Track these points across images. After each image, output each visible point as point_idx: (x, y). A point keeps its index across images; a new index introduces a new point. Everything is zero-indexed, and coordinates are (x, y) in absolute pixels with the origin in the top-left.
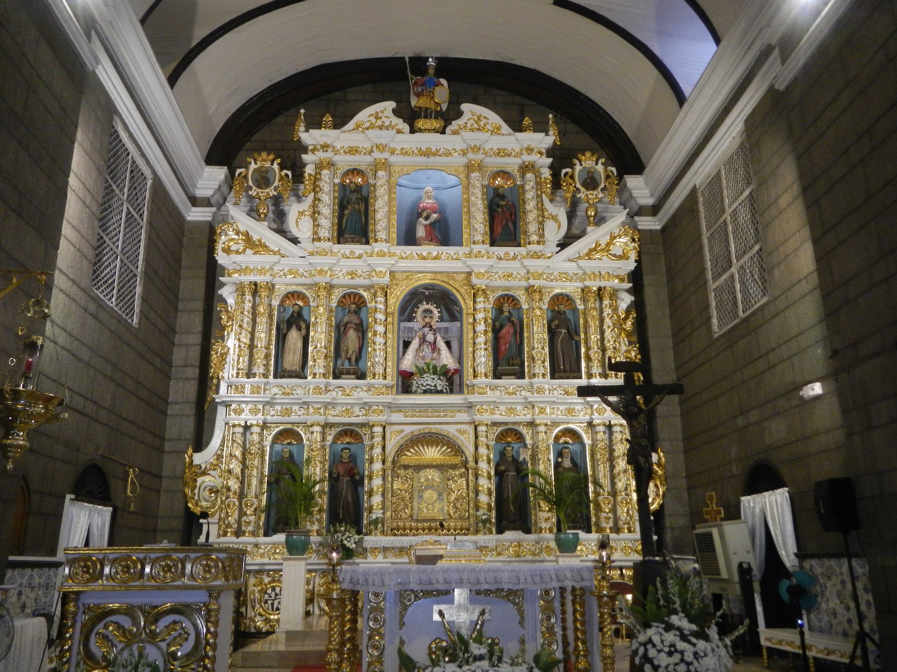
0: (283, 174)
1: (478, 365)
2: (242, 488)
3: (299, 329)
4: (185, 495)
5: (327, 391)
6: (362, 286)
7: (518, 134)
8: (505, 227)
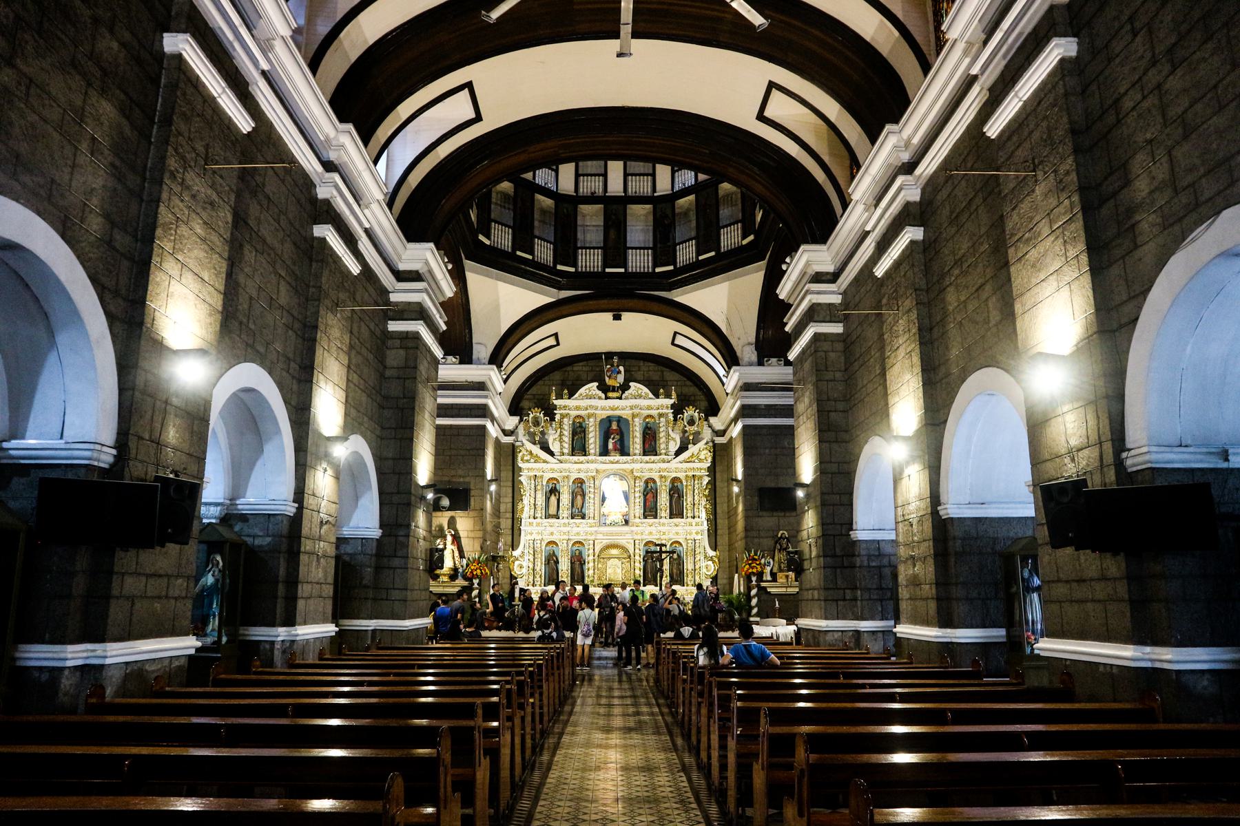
3: (555, 495)
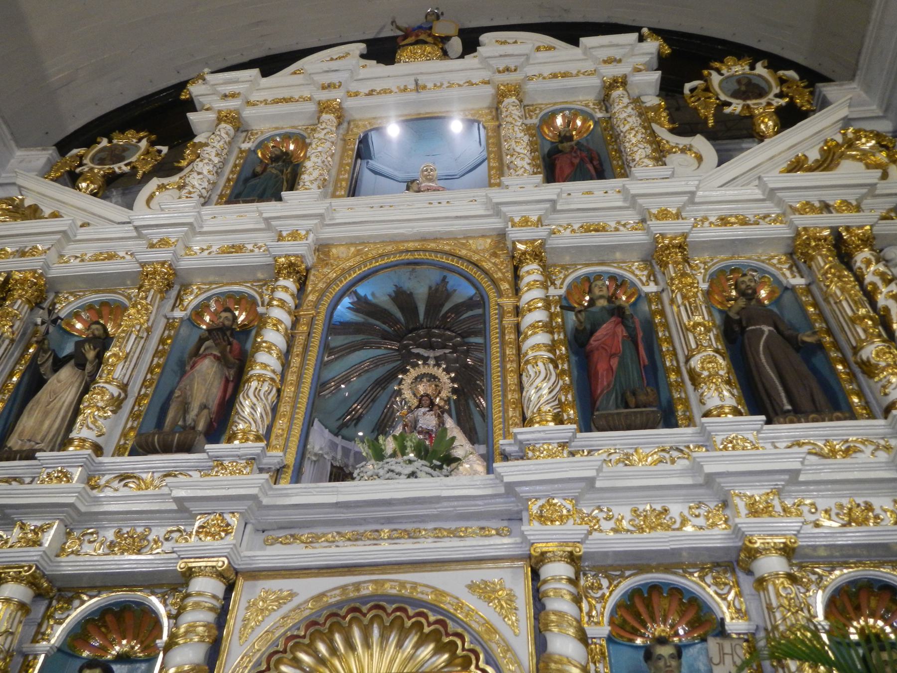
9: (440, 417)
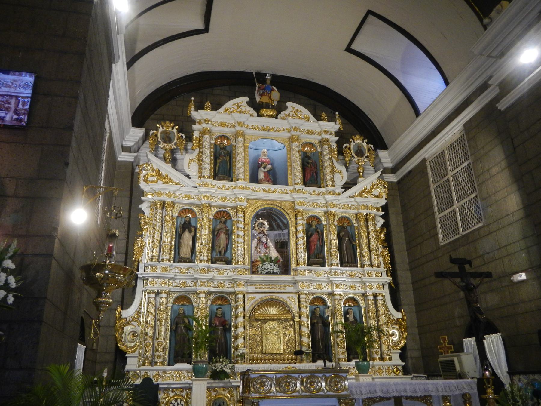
0: (179, 136)
1: (299, 258)
2: (154, 333)
3: (190, 232)
4: (116, 338)
5: (209, 271)
6: (230, 207)
7: (320, 122)
8: (312, 176)
9: (266, 238)
